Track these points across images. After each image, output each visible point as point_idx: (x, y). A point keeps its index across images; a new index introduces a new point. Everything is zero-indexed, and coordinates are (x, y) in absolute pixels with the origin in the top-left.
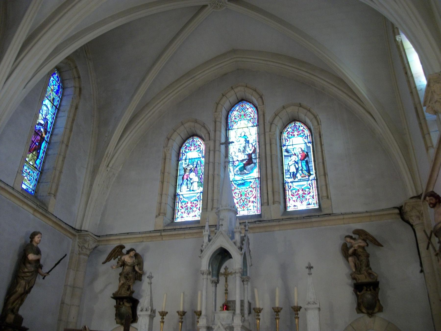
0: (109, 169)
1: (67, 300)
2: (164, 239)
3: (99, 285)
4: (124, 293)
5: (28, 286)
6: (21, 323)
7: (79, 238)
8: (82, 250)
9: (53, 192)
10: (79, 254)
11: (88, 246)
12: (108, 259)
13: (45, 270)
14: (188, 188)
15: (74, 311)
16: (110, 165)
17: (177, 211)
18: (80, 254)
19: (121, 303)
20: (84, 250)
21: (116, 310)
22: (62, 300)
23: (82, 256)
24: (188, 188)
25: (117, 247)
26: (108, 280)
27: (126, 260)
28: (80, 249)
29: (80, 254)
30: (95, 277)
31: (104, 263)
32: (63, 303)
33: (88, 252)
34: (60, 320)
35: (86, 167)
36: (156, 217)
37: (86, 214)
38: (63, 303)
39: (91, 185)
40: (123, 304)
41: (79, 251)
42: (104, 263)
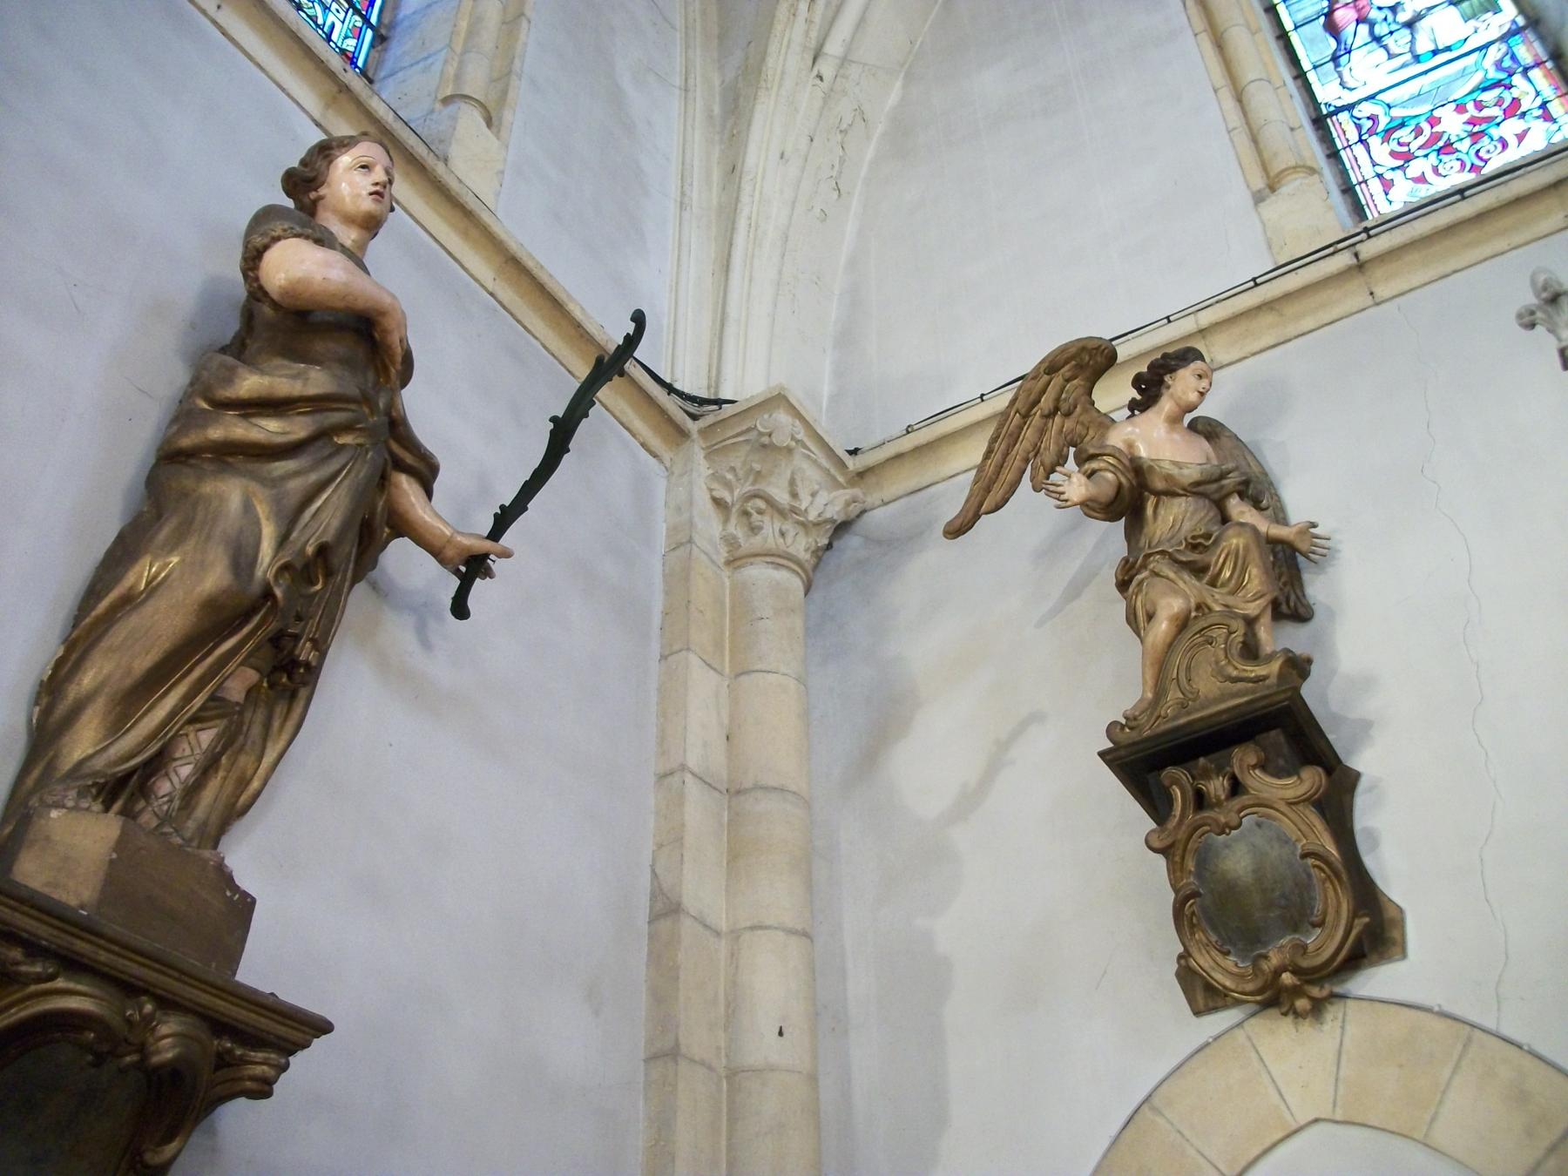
0: (827, 68)
1: (702, 890)
2: (1382, 291)
3: (930, 763)
4: (1213, 687)
5: (283, 541)
6: (233, 957)
7: (710, 454)
8: (754, 530)
9: (475, 82)
10: (735, 562)
11: (794, 495)
12: (989, 494)
13: (455, 507)
14: (1391, 56)
15: (772, 981)
16: (834, 48)
17: (1375, 186)
18: (735, 561)
19: (1216, 786)
20: (770, 528)
21: (1175, 870)
22: (657, 893)
23: (759, 573)
24: (1391, 56)
25: (1051, 366)
26: (1026, 655)
27: (1143, 452)
28: (736, 528)
29: (735, 561)
30: (885, 719)
31: (957, 530)
32: (666, 908)
33: (801, 546)
34: (665, 1054)
35: (678, 81)
36: (1258, 198)
37: (733, 312)
38: (666, 908)
39: (733, 171)
40: (1236, 788)
41: (731, 542)
42: (957, 530)
